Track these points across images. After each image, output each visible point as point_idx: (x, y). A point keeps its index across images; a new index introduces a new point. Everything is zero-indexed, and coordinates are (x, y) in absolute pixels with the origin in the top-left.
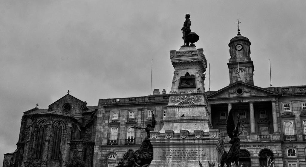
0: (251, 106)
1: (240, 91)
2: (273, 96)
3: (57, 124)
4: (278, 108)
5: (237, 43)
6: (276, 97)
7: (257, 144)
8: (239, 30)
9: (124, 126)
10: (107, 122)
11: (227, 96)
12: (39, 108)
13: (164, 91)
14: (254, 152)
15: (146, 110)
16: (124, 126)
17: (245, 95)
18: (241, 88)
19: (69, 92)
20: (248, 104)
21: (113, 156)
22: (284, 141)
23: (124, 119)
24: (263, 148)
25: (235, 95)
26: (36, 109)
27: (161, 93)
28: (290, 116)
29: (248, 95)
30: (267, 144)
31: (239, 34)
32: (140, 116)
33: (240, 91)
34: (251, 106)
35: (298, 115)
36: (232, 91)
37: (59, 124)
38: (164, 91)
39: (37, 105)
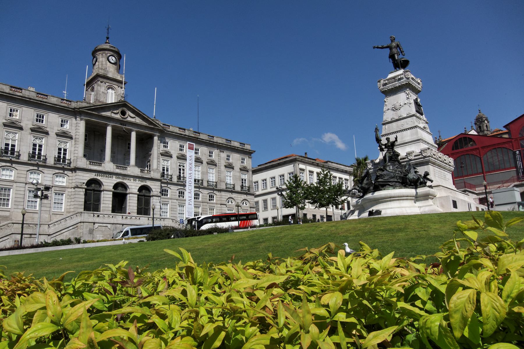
1: (123, 113)
8: (108, 38)
14: (133, 187)
17: (129, 119)
22: (164, 179)
24: (143, 184)
25: (118, 116)
33: (123, 113)
35: (174, 157)
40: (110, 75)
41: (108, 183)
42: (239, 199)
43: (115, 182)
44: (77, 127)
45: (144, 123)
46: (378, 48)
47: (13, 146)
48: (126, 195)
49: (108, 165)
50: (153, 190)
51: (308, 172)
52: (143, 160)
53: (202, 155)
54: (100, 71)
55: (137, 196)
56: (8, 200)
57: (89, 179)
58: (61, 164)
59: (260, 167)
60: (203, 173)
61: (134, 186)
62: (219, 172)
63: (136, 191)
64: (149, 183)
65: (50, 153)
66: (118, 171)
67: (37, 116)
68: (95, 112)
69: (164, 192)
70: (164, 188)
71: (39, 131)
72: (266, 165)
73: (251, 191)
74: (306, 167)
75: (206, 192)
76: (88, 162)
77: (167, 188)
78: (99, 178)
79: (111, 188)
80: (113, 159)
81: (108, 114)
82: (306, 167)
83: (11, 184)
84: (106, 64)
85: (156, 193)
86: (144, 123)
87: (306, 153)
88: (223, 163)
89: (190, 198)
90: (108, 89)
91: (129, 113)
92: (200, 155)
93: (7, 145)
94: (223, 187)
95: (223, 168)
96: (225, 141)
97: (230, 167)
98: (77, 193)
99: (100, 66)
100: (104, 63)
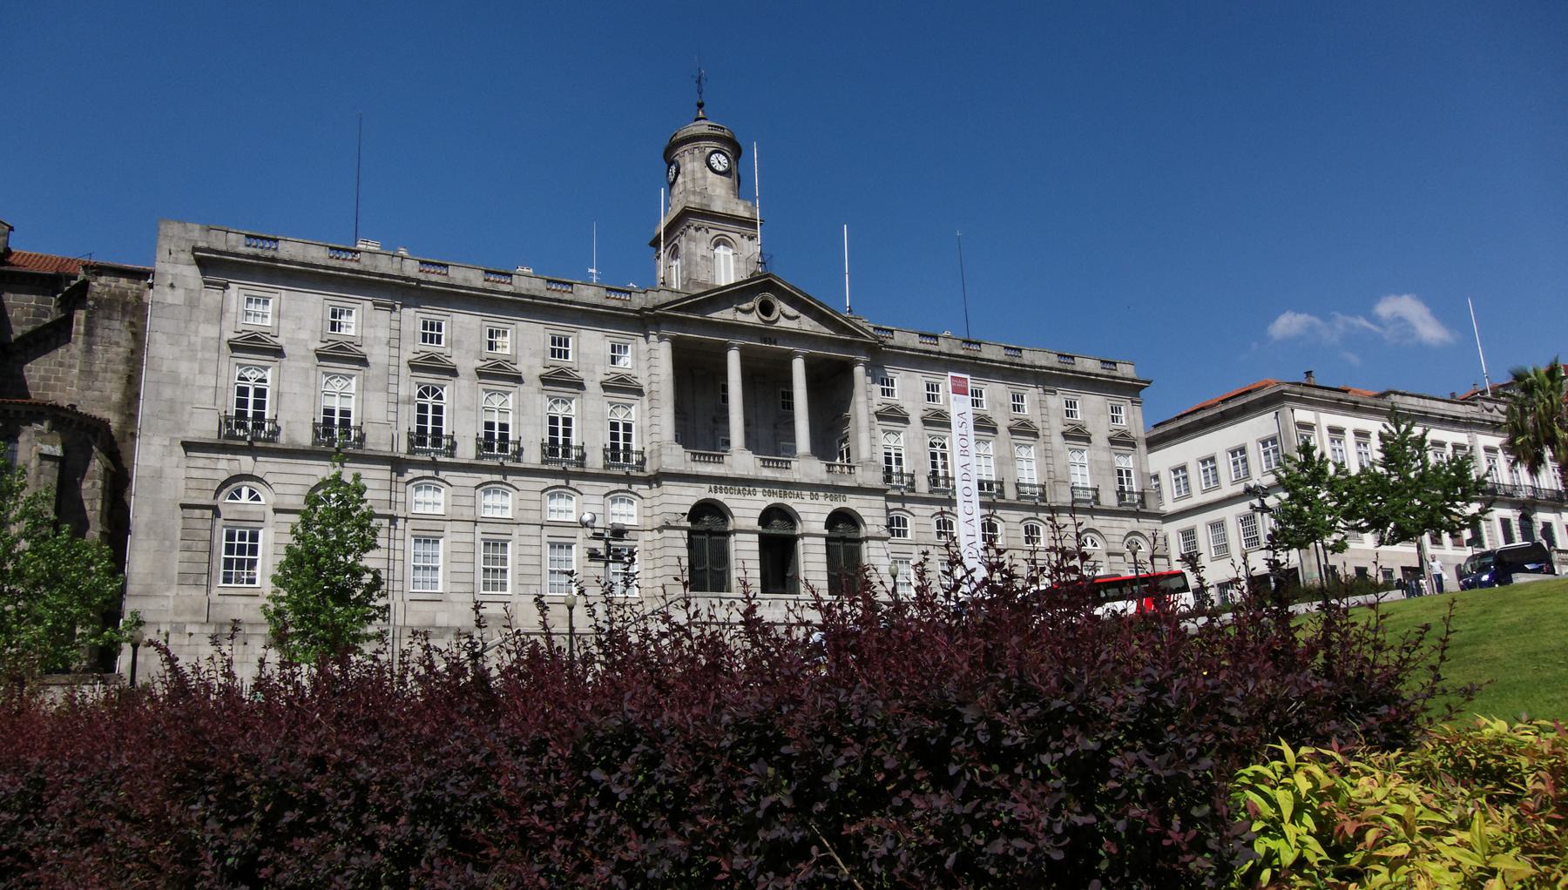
9: (303, 365)
10: (212, 331)
14: (812, 517)
16: (303, 365)
17: (783, 323)
21: (245, 491)
22: (894, 488)
23: (304, 335)
24: (837, 505)
25: (753, 319)
32: (383, 334)
35: (915, 418)
40: (718, 207)
41: (746, 509)
42: (1116, 531)
43: (764, 506)
44: (651, 360)
45: (825, 331)
47: (504, 427)
48: (794, 539)
49: (741, 460)
50: (867, 520)
51: (1325, 432)
52: (831, 437)
53: (994, 408)
54: (692, 198)
55: (823, 541)
56: (504, 571)
57: (693, 501)
58: (624, 468)
59: (1161, 430)
60: (1000, 462)
61: (813, 514)
62: (1048, 455)
63: (819, 526)
64: (853, 503)
65: (590, 437)
66: (768, 474)
67: (553, 343)
68: (694, 312)
69: (895, 526)
70: (894, 514)
71: (561, 381)
72: (1181, 423)
73: (1152, 505)
74: (1317, 418)
75: (1014, 517)
76: (689, 456)
77: (902, 514)
78: (720, 497)
79: (754, 523)
80: (751, 443)
81: (726, 315)
82: (1317, 418)
83: (507, 529)
84: (705, 178)
85: (875, 529)
86: (825, 331)
87: (1308, 374)
88: (1056, 425)
89: (971, 540)
90: (717, 245)
91: (781, 306)
92: (985, 408)
93: (490, 425)
94: (1064, 498)
95: (1057, 441)
96: (1054, 358)
97: (1077, 435)
98: (668, 543)
99: (690, 186)
100: (699, 175)
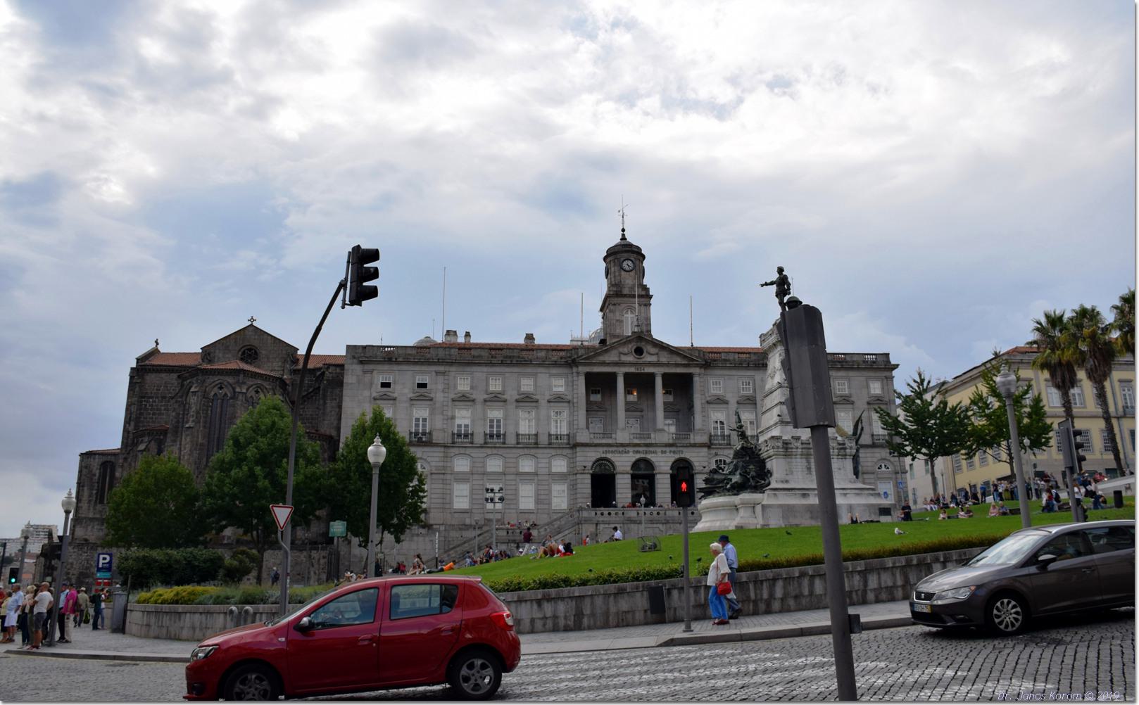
0: (659, 382)
1: (639, 351)
2: (697, 366)
3: (253, 393)
4: (708, 385)
5: (626, 255)
6: (701, 366)
7: (668, 449)
10: (367, 393)
11: (616, 359)
12: (162, 349)
13: (468, 335)
15: (452, 374)
17: (649, 359)
18: (642, 345)
19: (252, 320)
20: (652, 376)
23: (406, 391)
24: (677, 456)
25: (630, 359)
26: (154, 352)
27: (461, 339)
28: (720, 401)
29: (654, 359)
30: (685, 450)
31: (624, 238)
32: (440, 387)
33: (639, 351)
34: (659, 382)
36: (625, 350)
37: (257, 392)
38: (468, 335)
39: (157, 343)
41: (623, 463)
46: (766, 284)
50: (696, 464)
64: (688, 454)
78: (609, 456)
79: (629, 469)
